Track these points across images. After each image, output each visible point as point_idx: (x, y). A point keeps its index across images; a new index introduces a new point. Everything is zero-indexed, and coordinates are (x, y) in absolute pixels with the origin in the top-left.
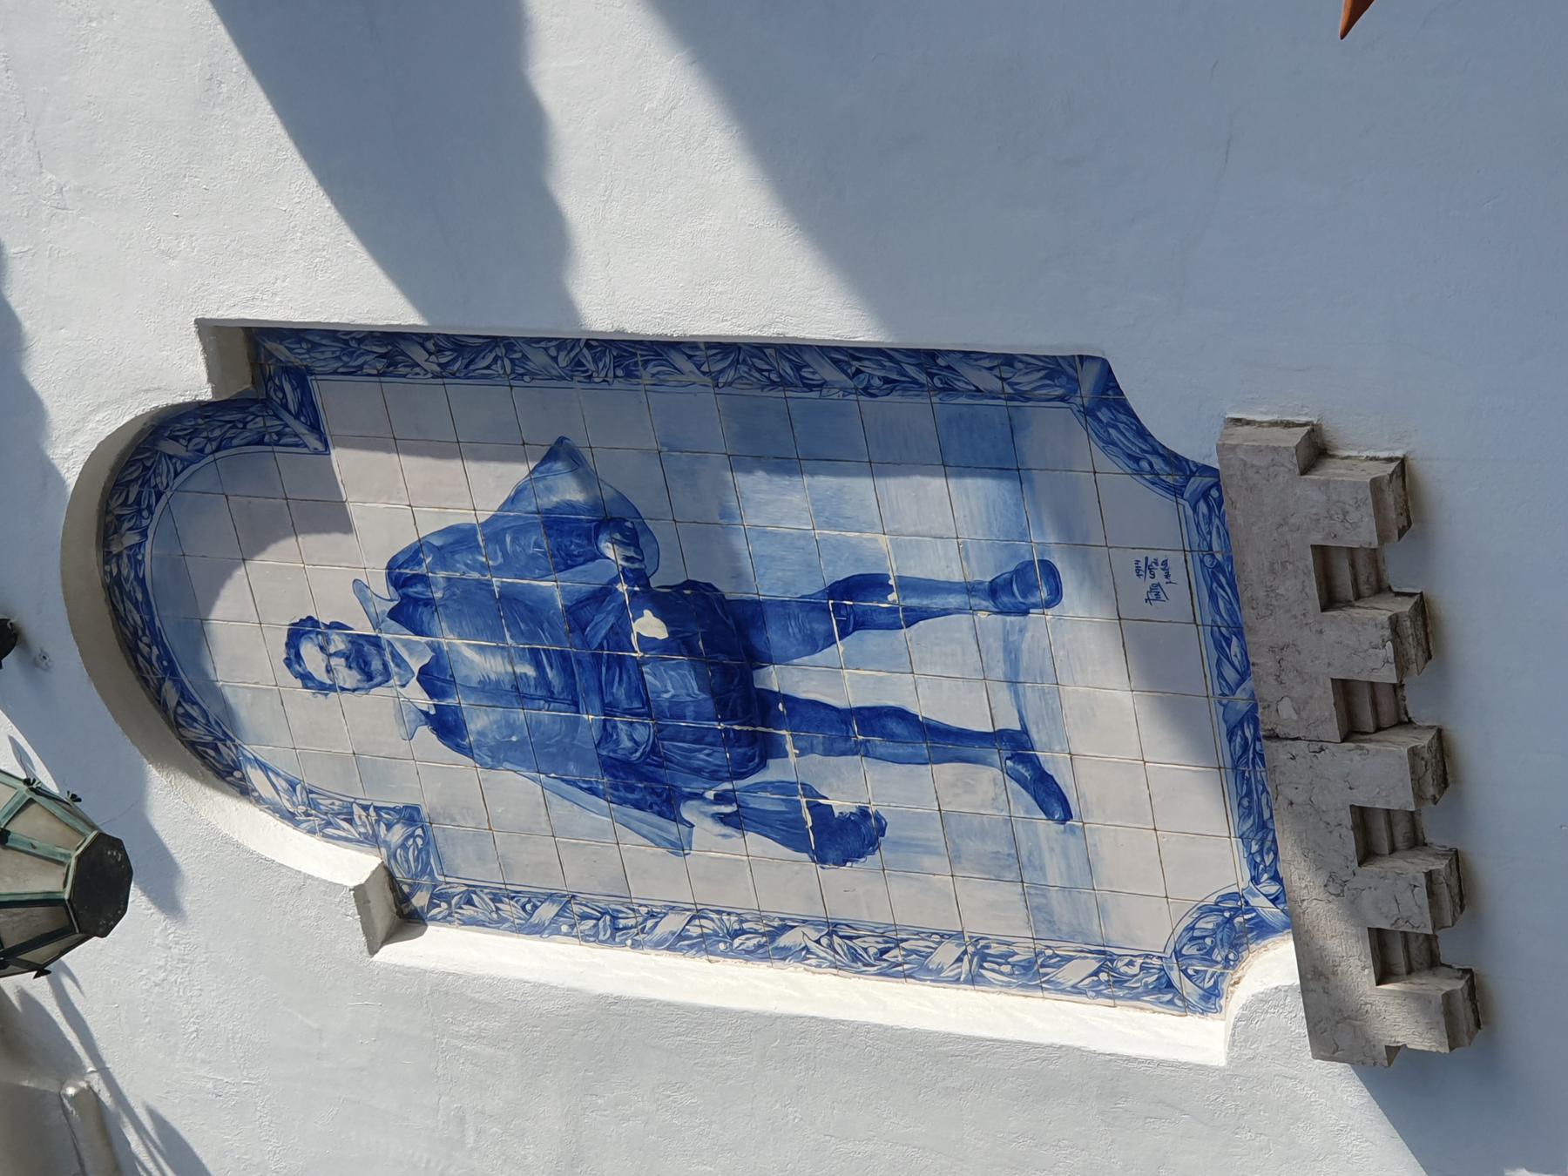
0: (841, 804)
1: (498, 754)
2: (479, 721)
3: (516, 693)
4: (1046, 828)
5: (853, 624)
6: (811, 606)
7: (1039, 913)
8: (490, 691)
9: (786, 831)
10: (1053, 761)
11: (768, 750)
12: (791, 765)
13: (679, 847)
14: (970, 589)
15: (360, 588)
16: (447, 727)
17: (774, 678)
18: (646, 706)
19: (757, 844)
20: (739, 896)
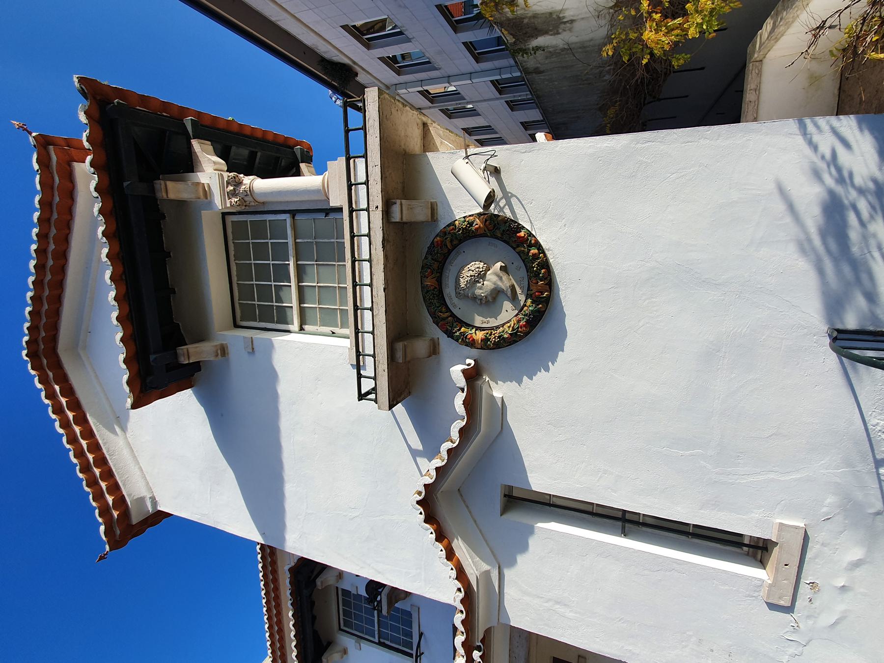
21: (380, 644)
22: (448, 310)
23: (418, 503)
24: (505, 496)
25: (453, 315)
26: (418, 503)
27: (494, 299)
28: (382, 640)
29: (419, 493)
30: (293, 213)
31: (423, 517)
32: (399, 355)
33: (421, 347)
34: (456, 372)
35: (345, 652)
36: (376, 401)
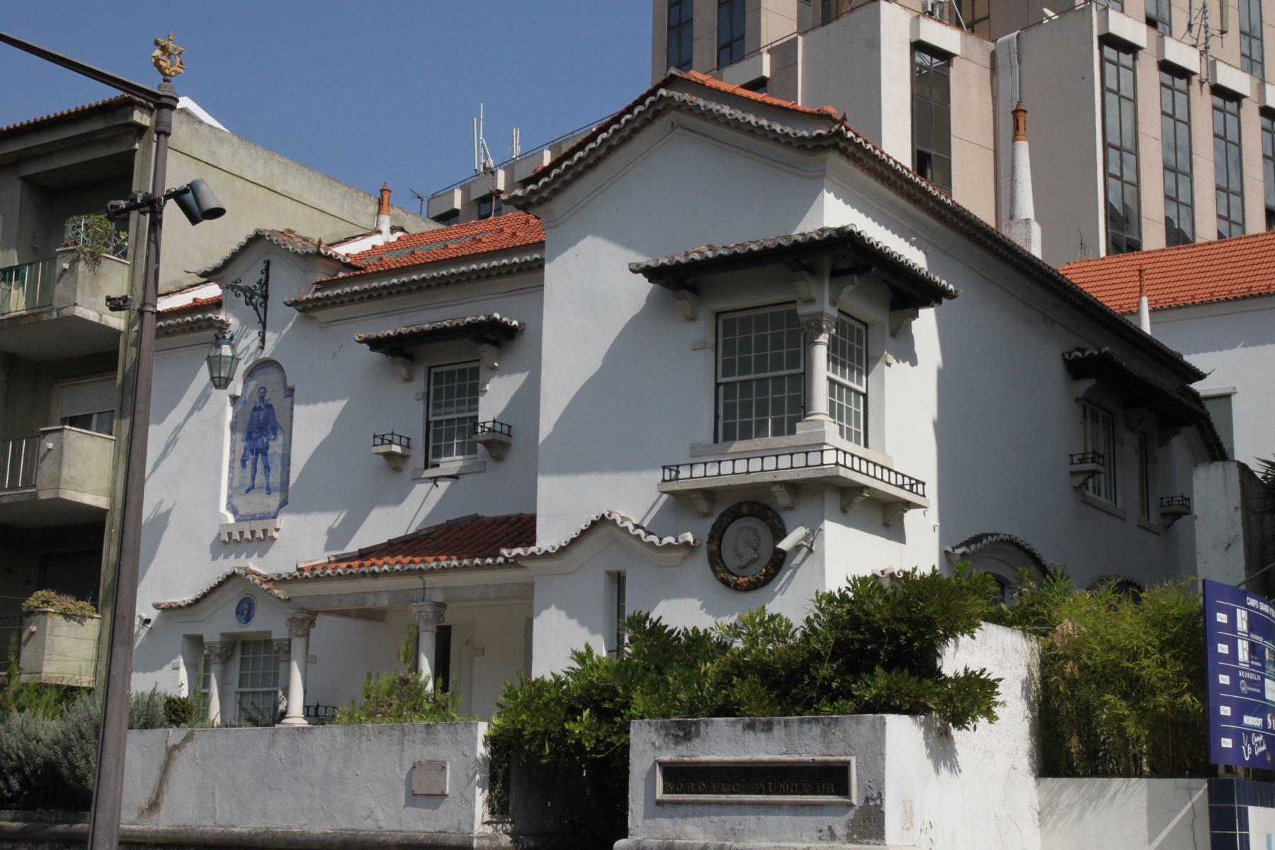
0: (247, 463)
1: (252, 417)
2: (255, 414)
3: (258, 420)
4: (245, 489)
5: (265, 467)
6: (267, 462)
7: (237, 488)
8: (258, 416)
9: (244, 455)
10: (252, 491)
11: (253, 454)
12: (252, 457)
13: (242, 440)
14: (268, 483)
15: (269, 399)
16: (255, 409)
17: (260, 455)
18: (257, 438)
19: (243, 451)
20: (237, 448)
21: (428, 423)
22: (730, 523)
23: (603, 515)
24: (619, 573)
25: (727, 527)
26: (603, 515)
27: (738, 555)
28: (432, 425)
29: (609, 515)
30: (804, 374)
31: (595, 519)
32: (693, 496)
33: (703, 506)
34: (689, 537)
35: (409, 379)
36: (664, 481)
